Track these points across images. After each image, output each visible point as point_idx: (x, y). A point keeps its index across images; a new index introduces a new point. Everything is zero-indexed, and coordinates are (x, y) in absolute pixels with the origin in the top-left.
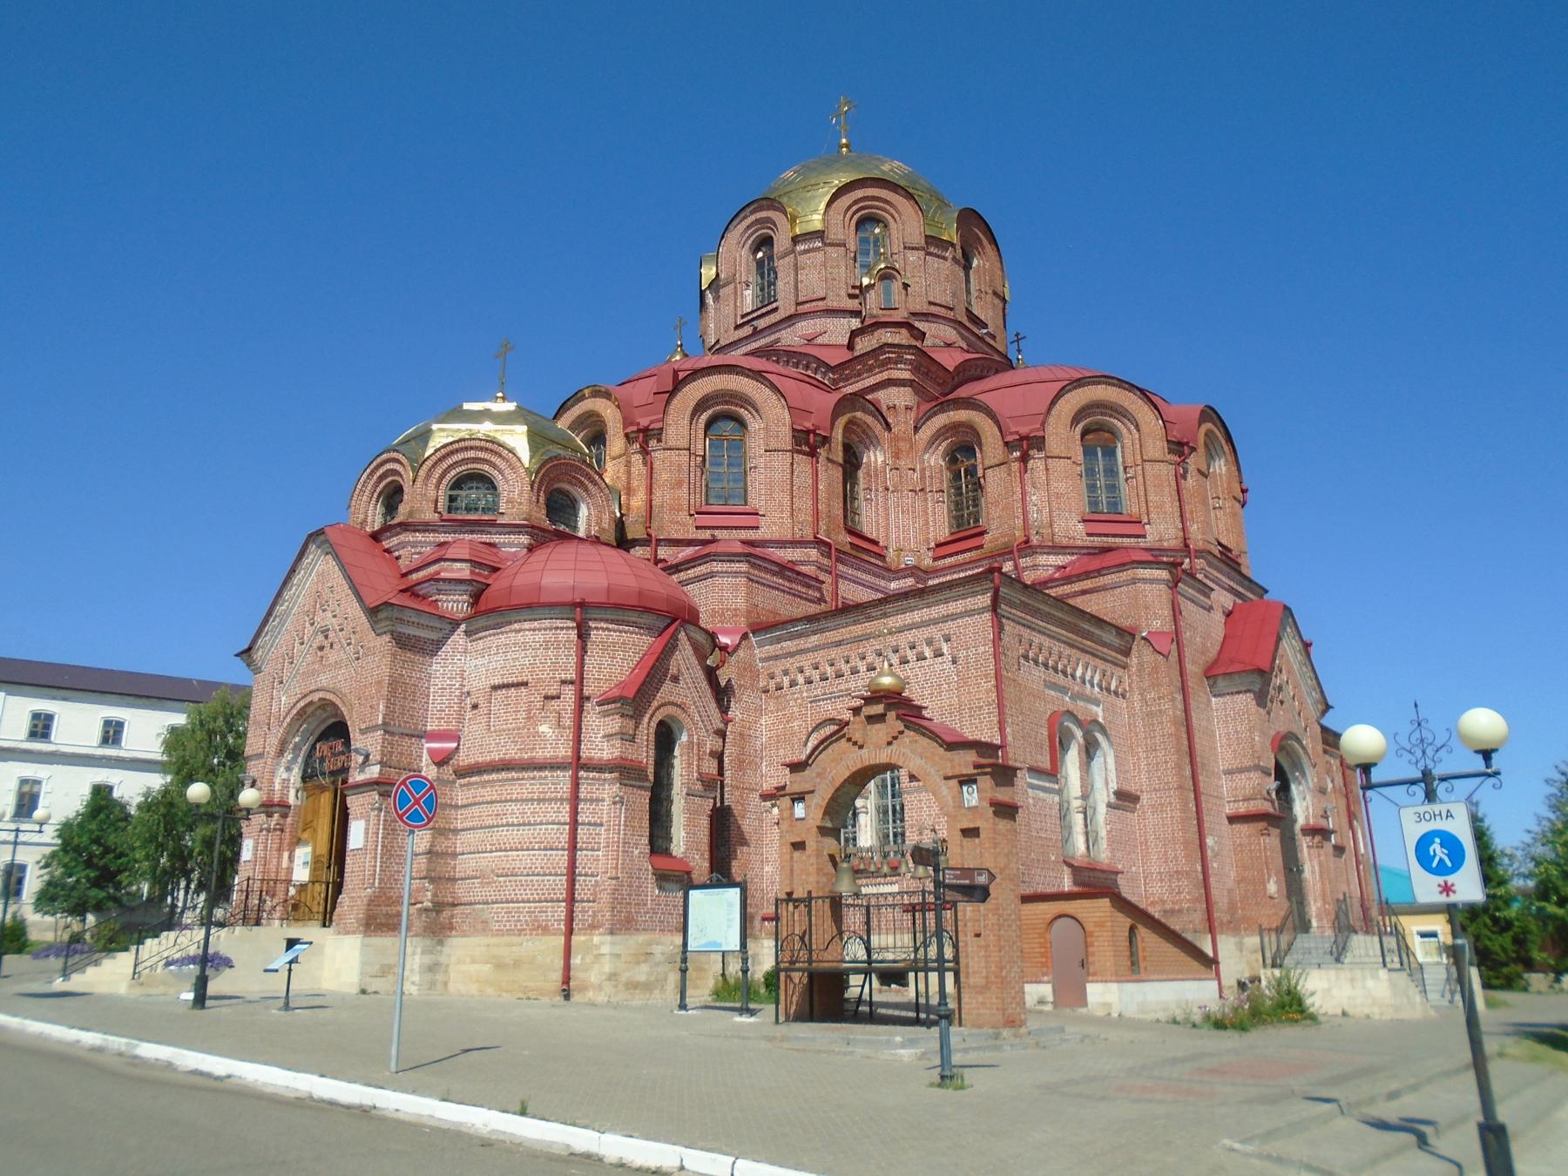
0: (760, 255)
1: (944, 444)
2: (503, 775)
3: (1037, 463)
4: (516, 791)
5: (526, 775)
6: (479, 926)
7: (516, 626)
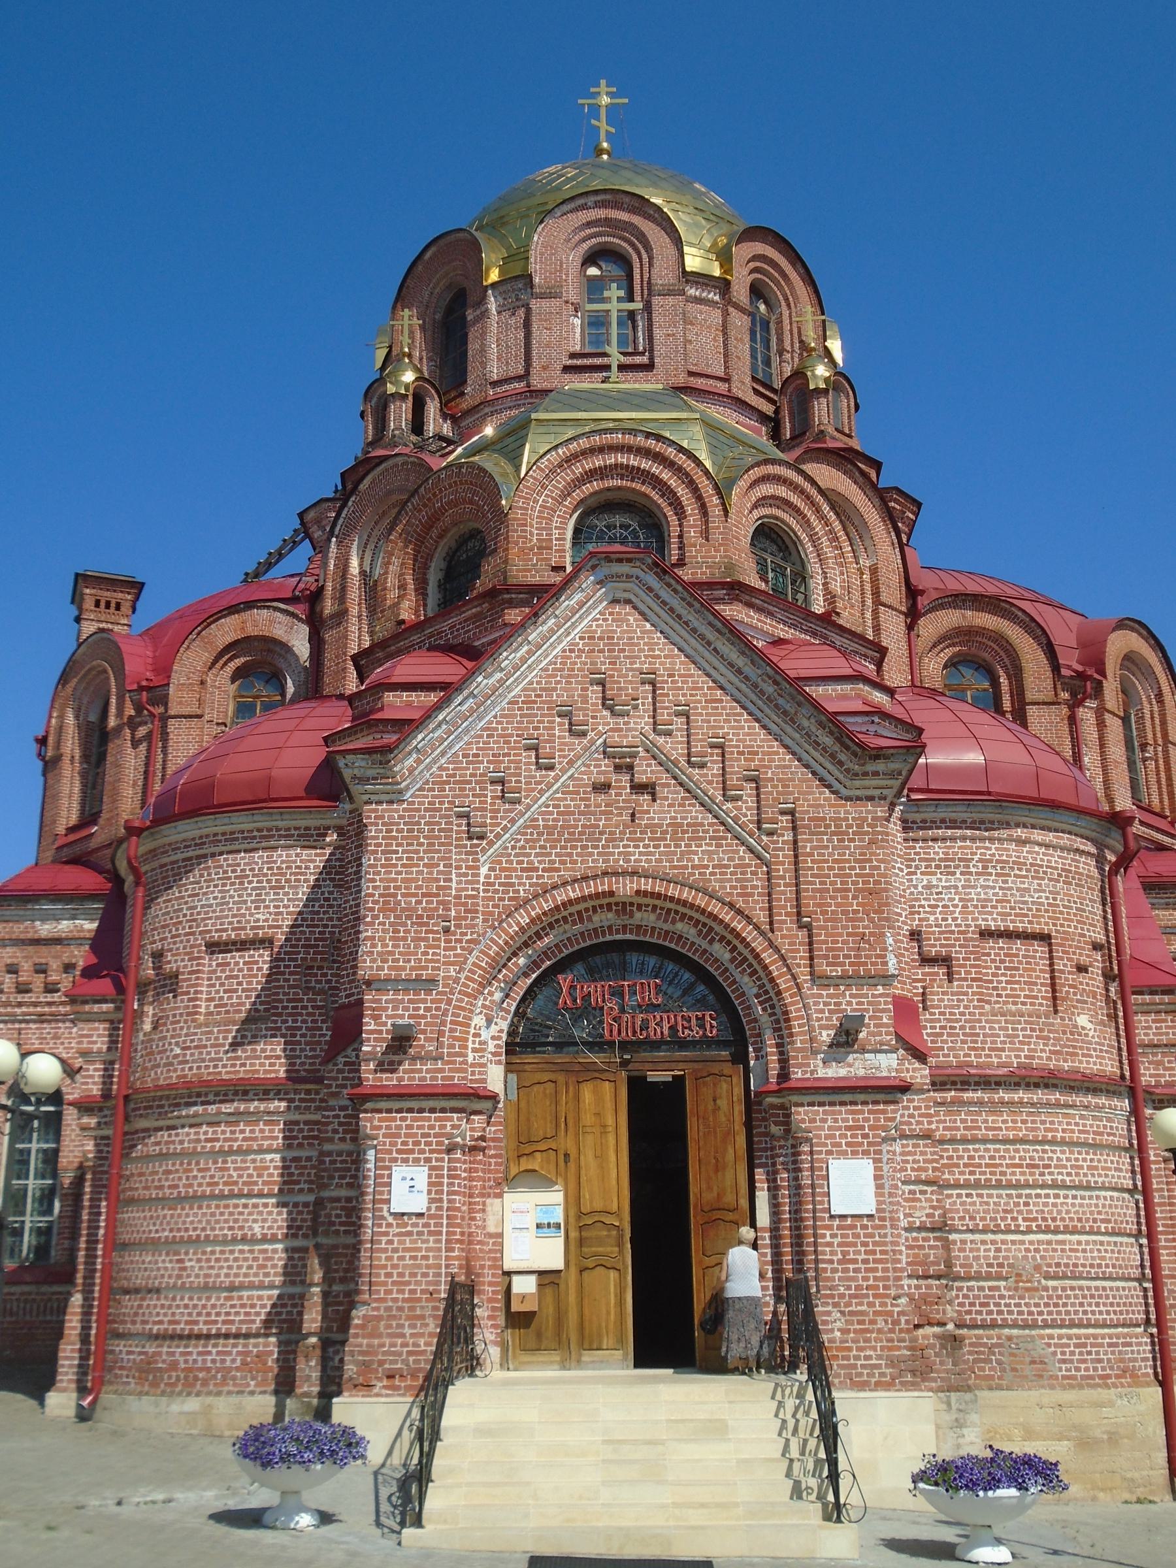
0: (593, 271)
1: (949, 652)
2: (1039, 1095)
3: (1087, 714)
4: (1061, 1124)
5: (1078, 1099)
6: (1028, 1371)
7: (1019, 832)
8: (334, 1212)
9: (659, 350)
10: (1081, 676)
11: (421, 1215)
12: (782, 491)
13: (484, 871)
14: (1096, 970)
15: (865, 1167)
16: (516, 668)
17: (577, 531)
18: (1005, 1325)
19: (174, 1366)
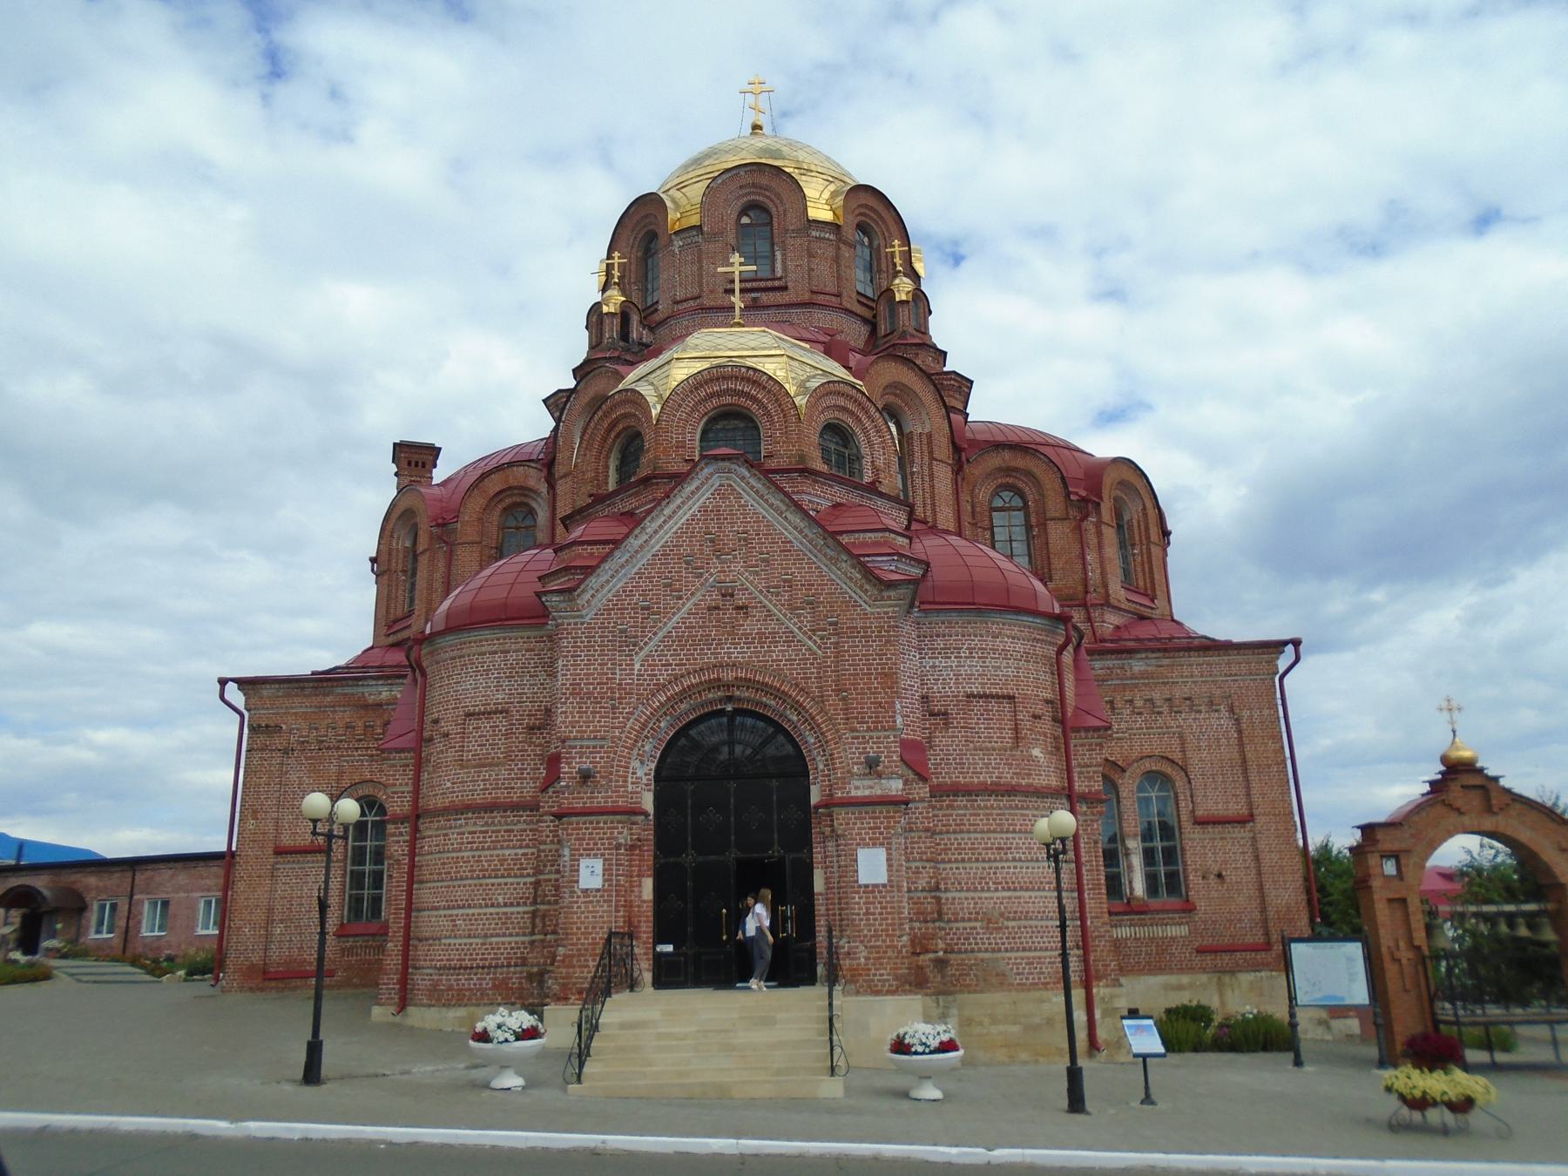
0: (745, 220)
3: (1089, 524)
6: (994, 980)
8: (548, 889)
9: (792, 276)
10: (1083, 500)
11: (598, 890)
12: (841, 402)
13: (637, 666)
14: (1048, 717)
15: (880, 854)
16: (656, 532)
17: (704, 432)
18: (980, 950)
19: (450, 988)
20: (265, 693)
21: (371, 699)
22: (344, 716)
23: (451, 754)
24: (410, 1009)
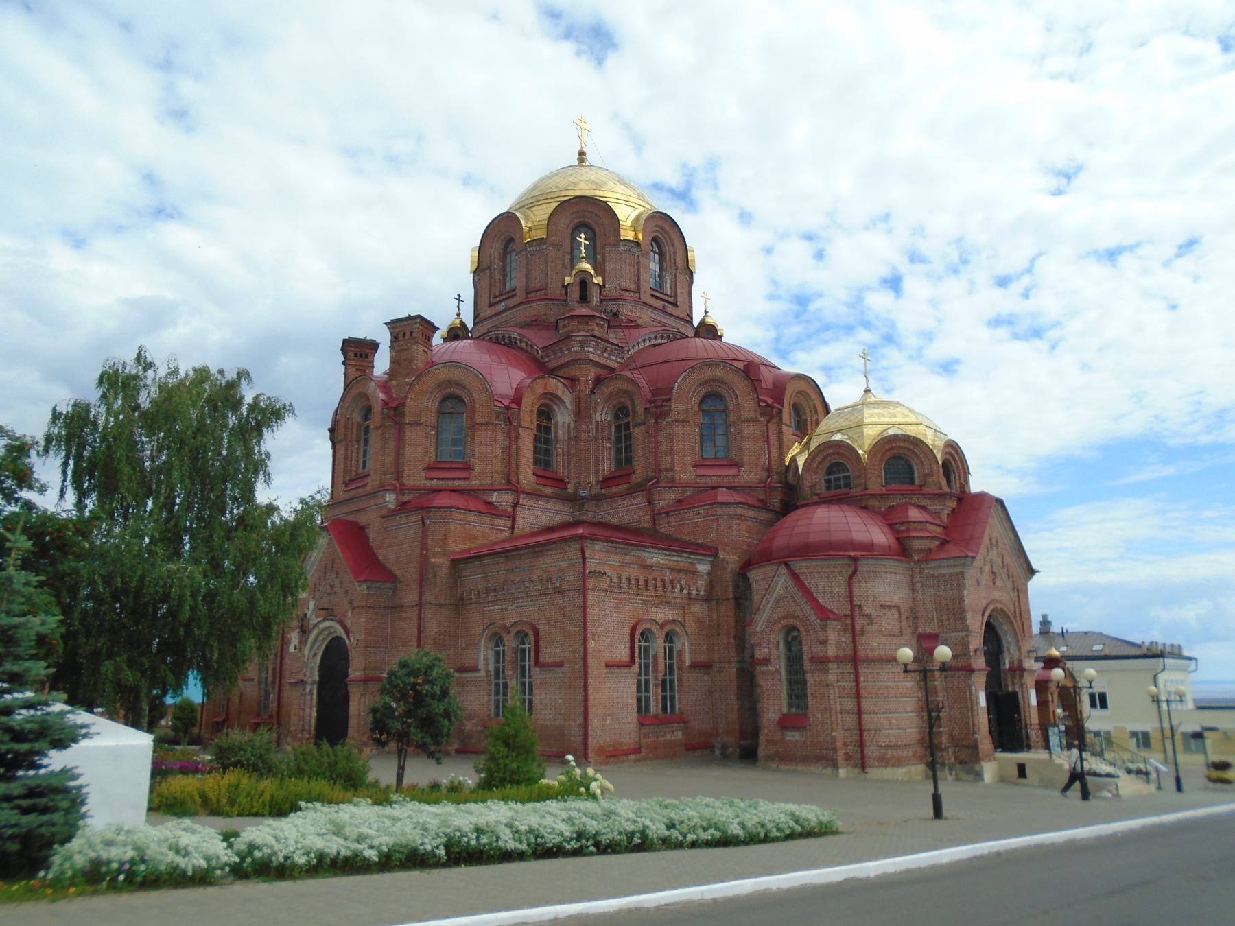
20: (597, 547)
21: (649, 561)
22: (633, 572)
23: (874, 627)
24: (868, 770)
